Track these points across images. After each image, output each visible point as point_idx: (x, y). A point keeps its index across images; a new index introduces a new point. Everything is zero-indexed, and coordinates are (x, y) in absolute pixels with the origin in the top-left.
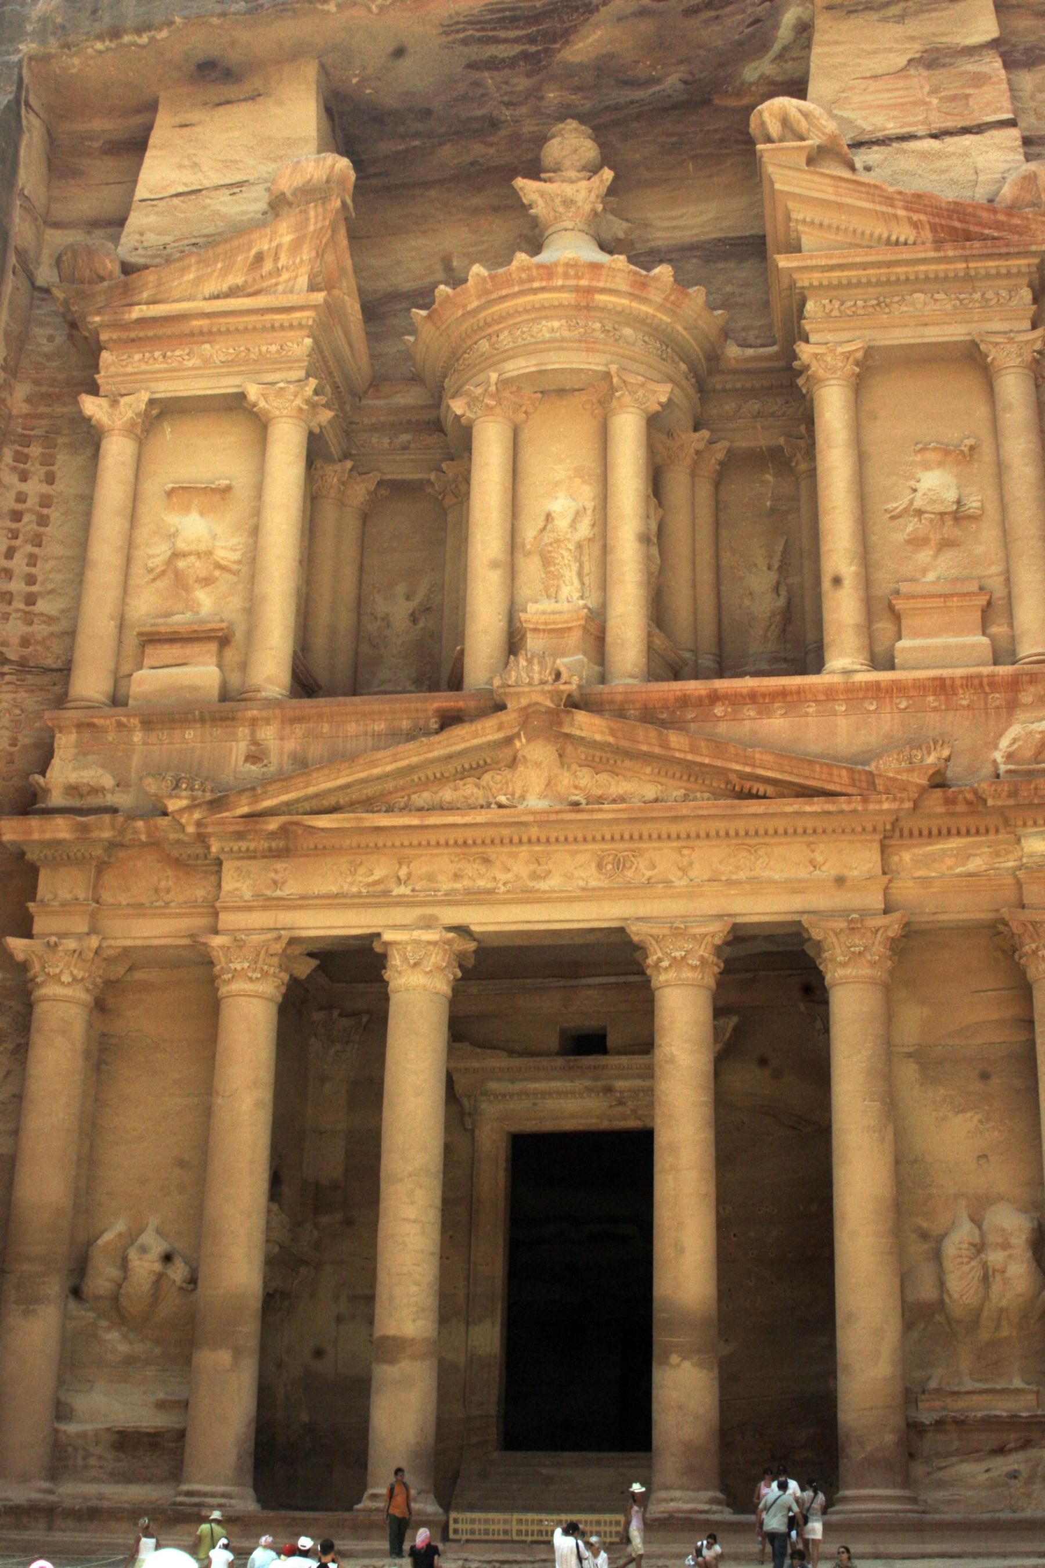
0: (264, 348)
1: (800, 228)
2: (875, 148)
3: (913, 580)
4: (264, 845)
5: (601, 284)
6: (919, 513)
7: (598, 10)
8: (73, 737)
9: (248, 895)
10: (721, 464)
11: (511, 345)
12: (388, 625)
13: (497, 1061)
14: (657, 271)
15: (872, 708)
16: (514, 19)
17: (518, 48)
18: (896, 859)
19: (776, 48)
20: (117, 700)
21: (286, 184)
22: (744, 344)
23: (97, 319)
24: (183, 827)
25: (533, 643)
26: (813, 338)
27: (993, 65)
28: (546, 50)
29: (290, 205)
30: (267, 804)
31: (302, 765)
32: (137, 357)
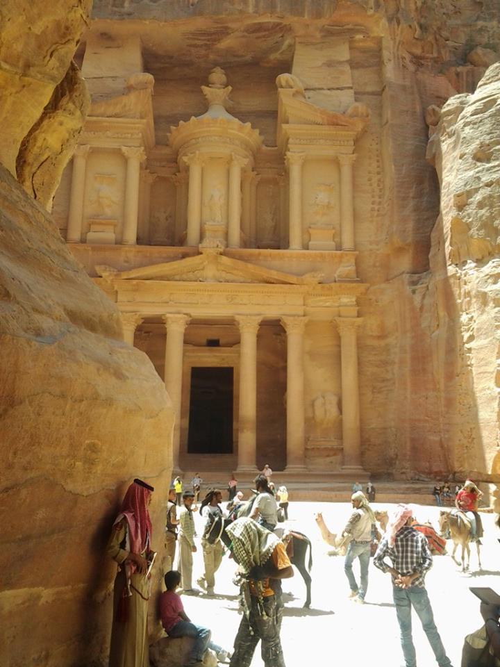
6: (318, 205)
10: (259, 182)
12: (159, 220)
13: (190, 347)
14: (246, 124)
16: (205, 34)
17: (205, 42)
19: (280, 51)
20: (83, 241)
25: (208, 234)
26: (291, 150)
27: (347, 68)
30: (133, 276)
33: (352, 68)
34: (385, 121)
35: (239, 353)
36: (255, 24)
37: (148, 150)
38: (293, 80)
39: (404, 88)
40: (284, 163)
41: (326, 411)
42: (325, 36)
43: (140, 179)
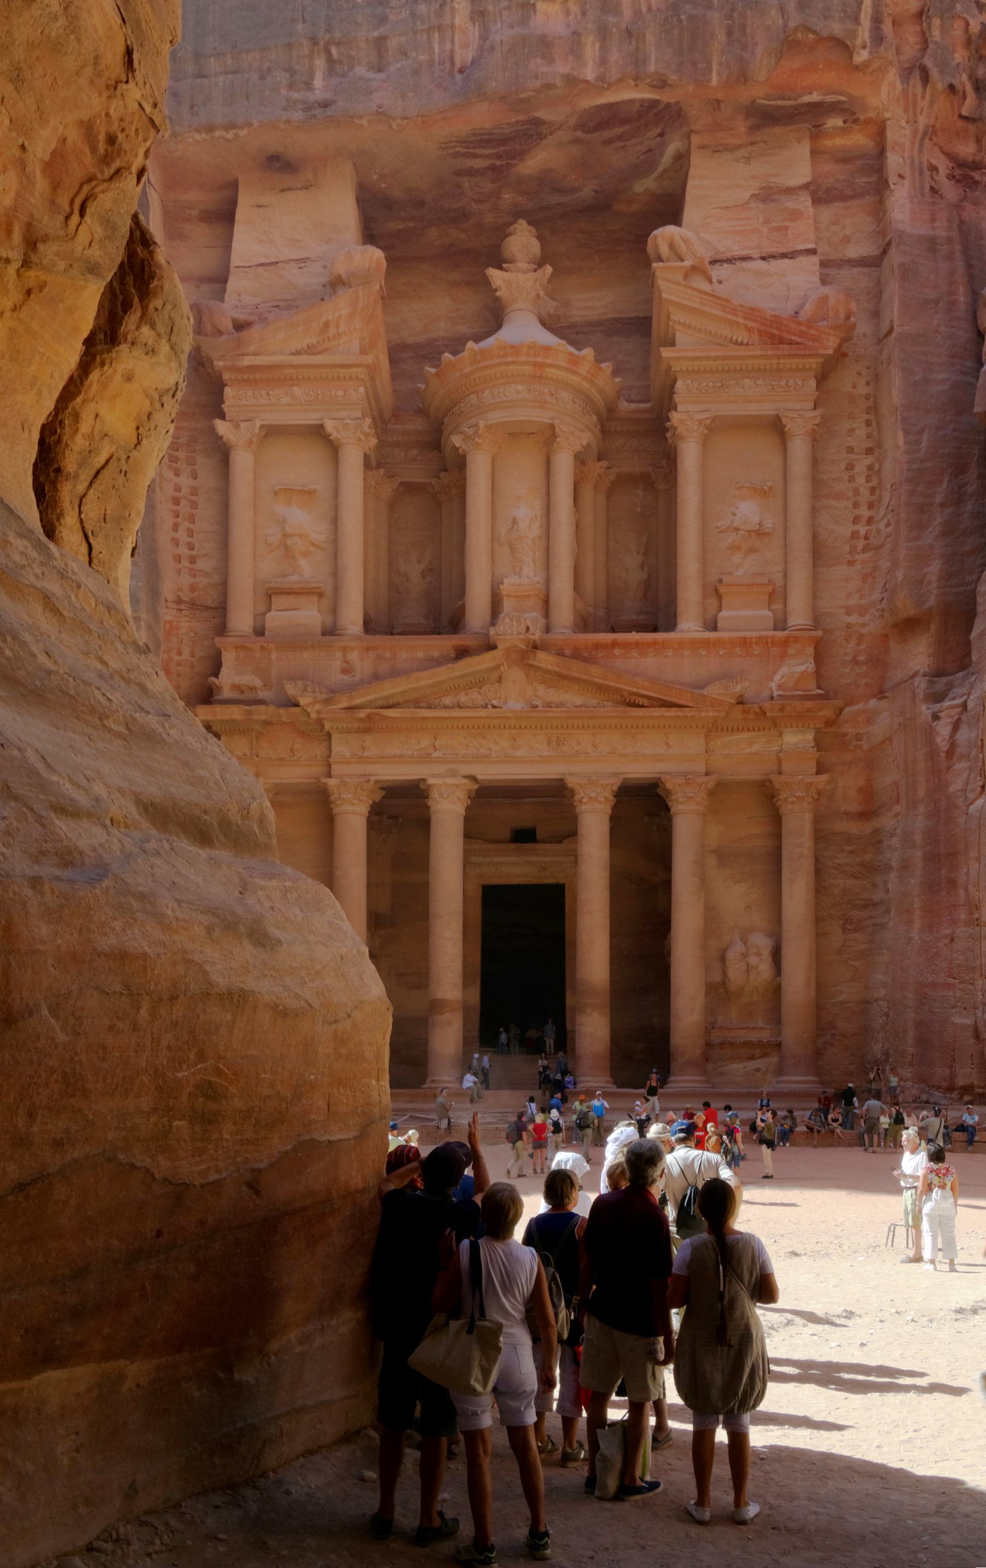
0: (333, 393)
1: (676, 326)
2: (726, 265)
3: (731, 574)
4: (356, 725)
5: (549, 361)
6: (737, 530)
7: (545, 137)
8: (234, 654)
9: (348, 755)
11: (491, 401)
15: (704, 653)
18: (712, 743)
21: (341, 269)
22: (630, 401)
23: (221, 363)
24: (309, 715)
25: (508, 604)
26: (680, 408)
27: (804, 202)
28: (507, 164)
29: (344, 284)
30: (357, 701)
31: (376, 677)
32: (250, 393)
33: (816, 201)
34: (885, 327)
35: (576, 856)
36: (600, 108)
37: (382, 423)
38: (685, 241)
39: (931, 244)
40: (666, 439)
41: (749, 966)
42: (755, 128)
43: (366, 488)
